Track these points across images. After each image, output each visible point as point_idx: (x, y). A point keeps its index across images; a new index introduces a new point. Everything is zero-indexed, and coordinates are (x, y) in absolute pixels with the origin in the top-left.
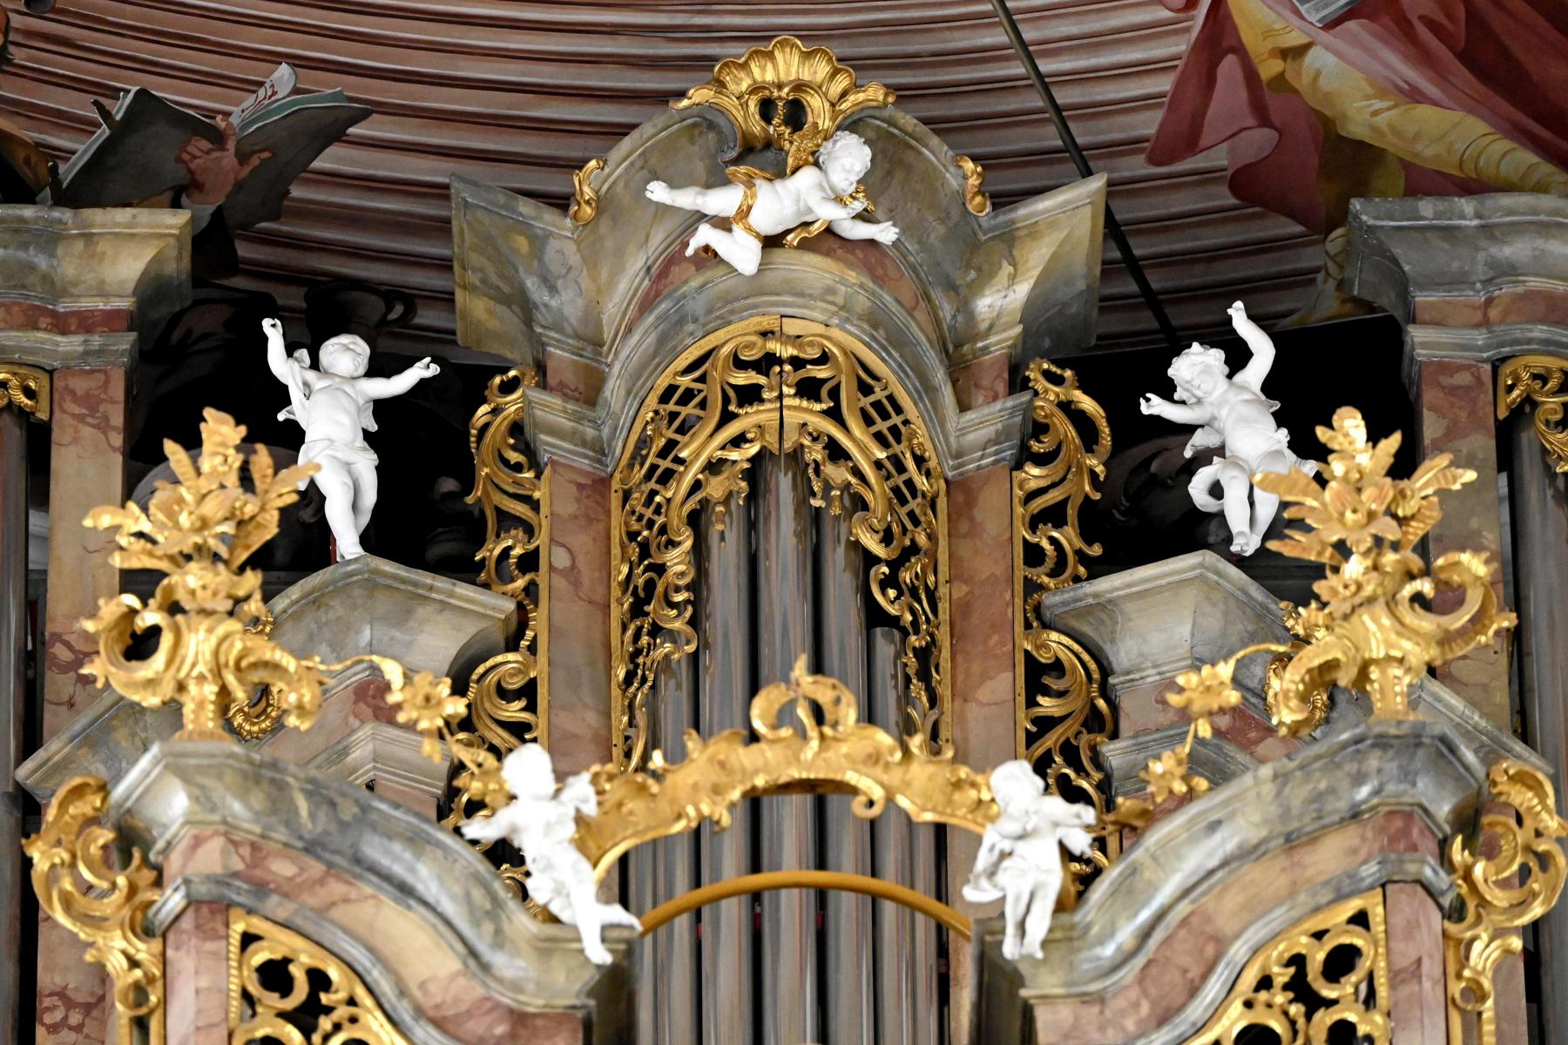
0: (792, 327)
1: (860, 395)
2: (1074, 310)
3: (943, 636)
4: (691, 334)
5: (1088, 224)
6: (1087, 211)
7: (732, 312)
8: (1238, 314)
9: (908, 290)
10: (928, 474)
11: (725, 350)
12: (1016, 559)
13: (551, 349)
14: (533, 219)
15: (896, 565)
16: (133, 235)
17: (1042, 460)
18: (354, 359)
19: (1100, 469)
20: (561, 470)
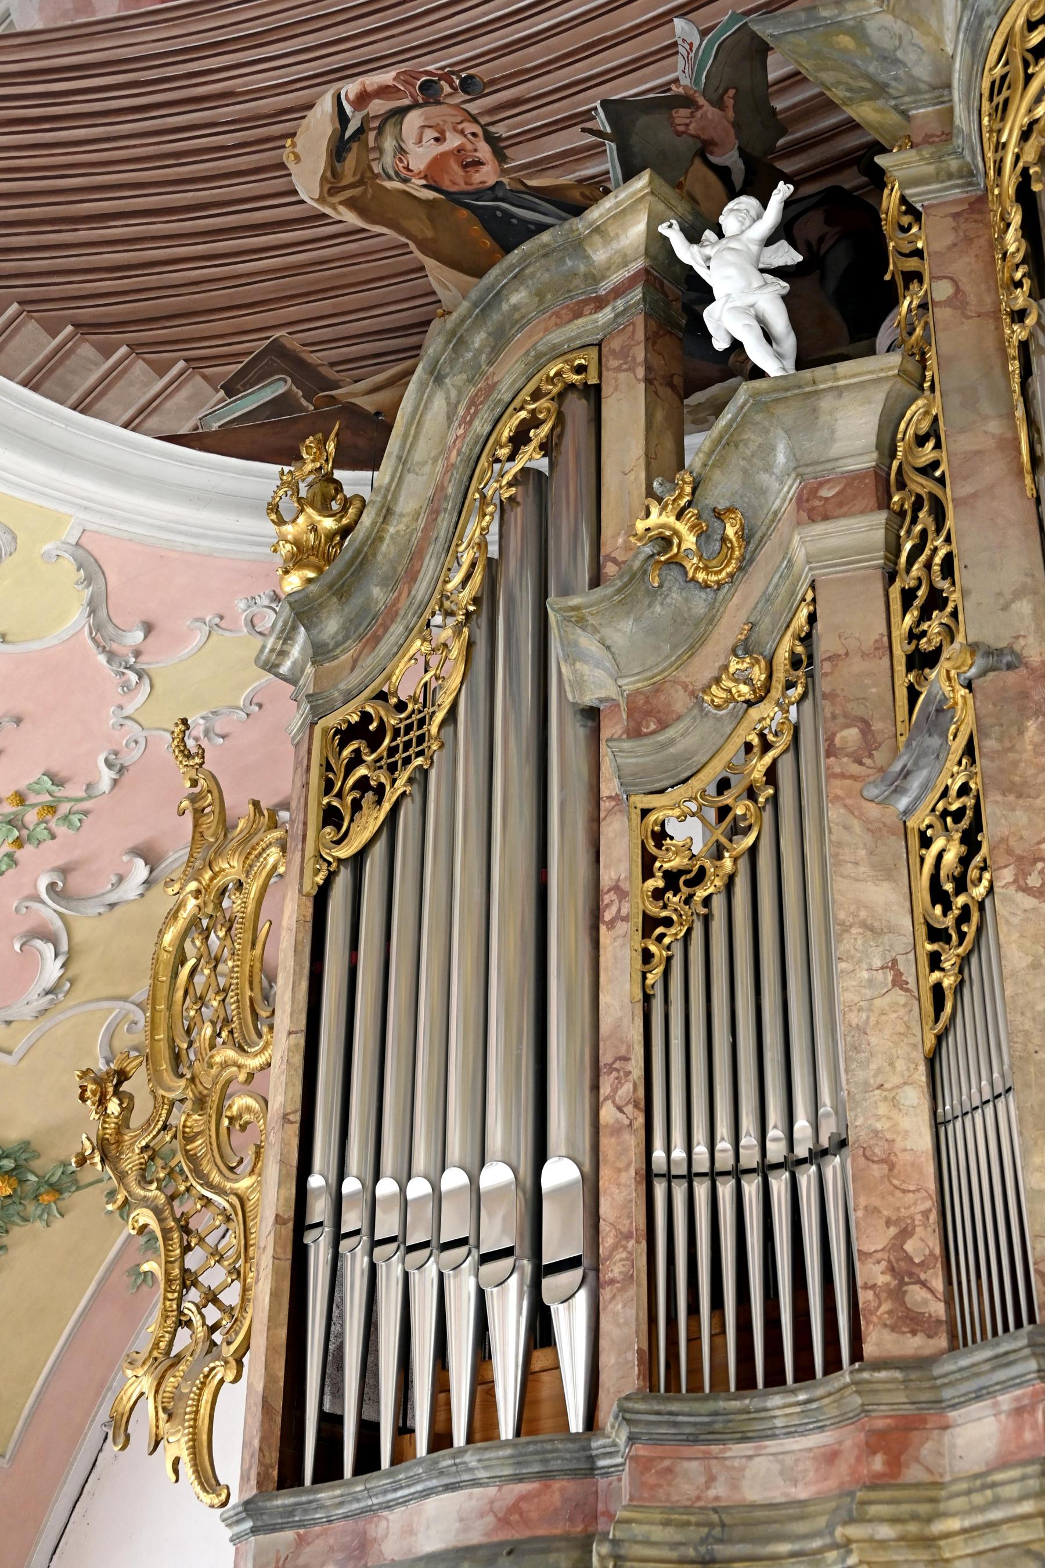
4: (990, 27)
11: (1021, 21)
13: (914, 112)
14: (839, 15)
18: (737, 217)
20: (932, 211)
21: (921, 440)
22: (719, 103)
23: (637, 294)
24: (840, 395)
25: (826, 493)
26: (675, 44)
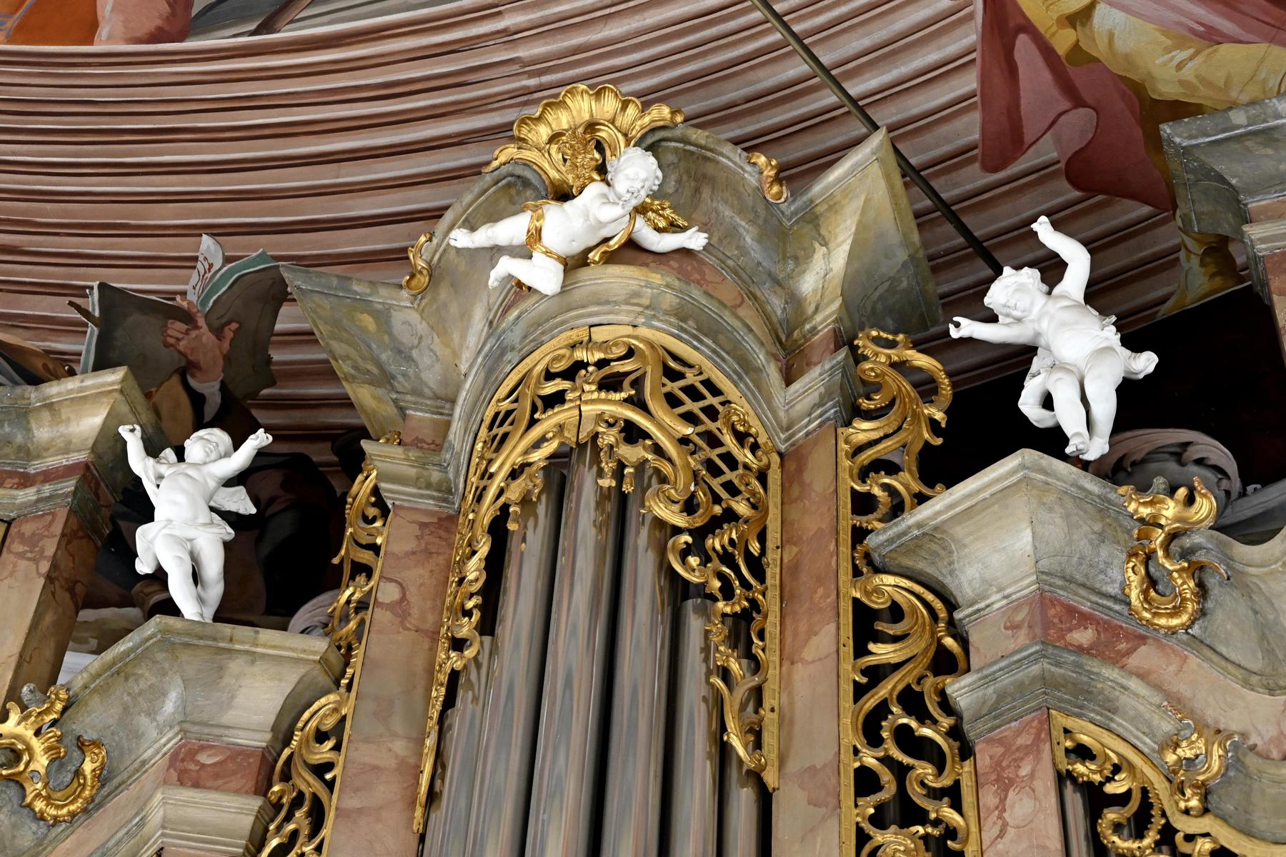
0: (599, 335)
1: (665, 380)
2: (905, 284)
3: (771, 603)
4: (510, 362)
5: (882, 184)
6: (875, 169)
7: (543, 333)
8: (1043, 229)
9: (729, 291)
10: (755, 448)
11: (540, 367)
12: (841, 510)
13: (411, 412)
14: (370, 295)
15: (700, 534)
16: (84, 399)
17: (869, 416)
18: (205, 447)
19: (939, 416)
20: (402, 513)
21: (321, 737)
22: (218, 332)
23: (69, 485)
24: (253, 662)
25: (204, 758)
26: (196, 259)
